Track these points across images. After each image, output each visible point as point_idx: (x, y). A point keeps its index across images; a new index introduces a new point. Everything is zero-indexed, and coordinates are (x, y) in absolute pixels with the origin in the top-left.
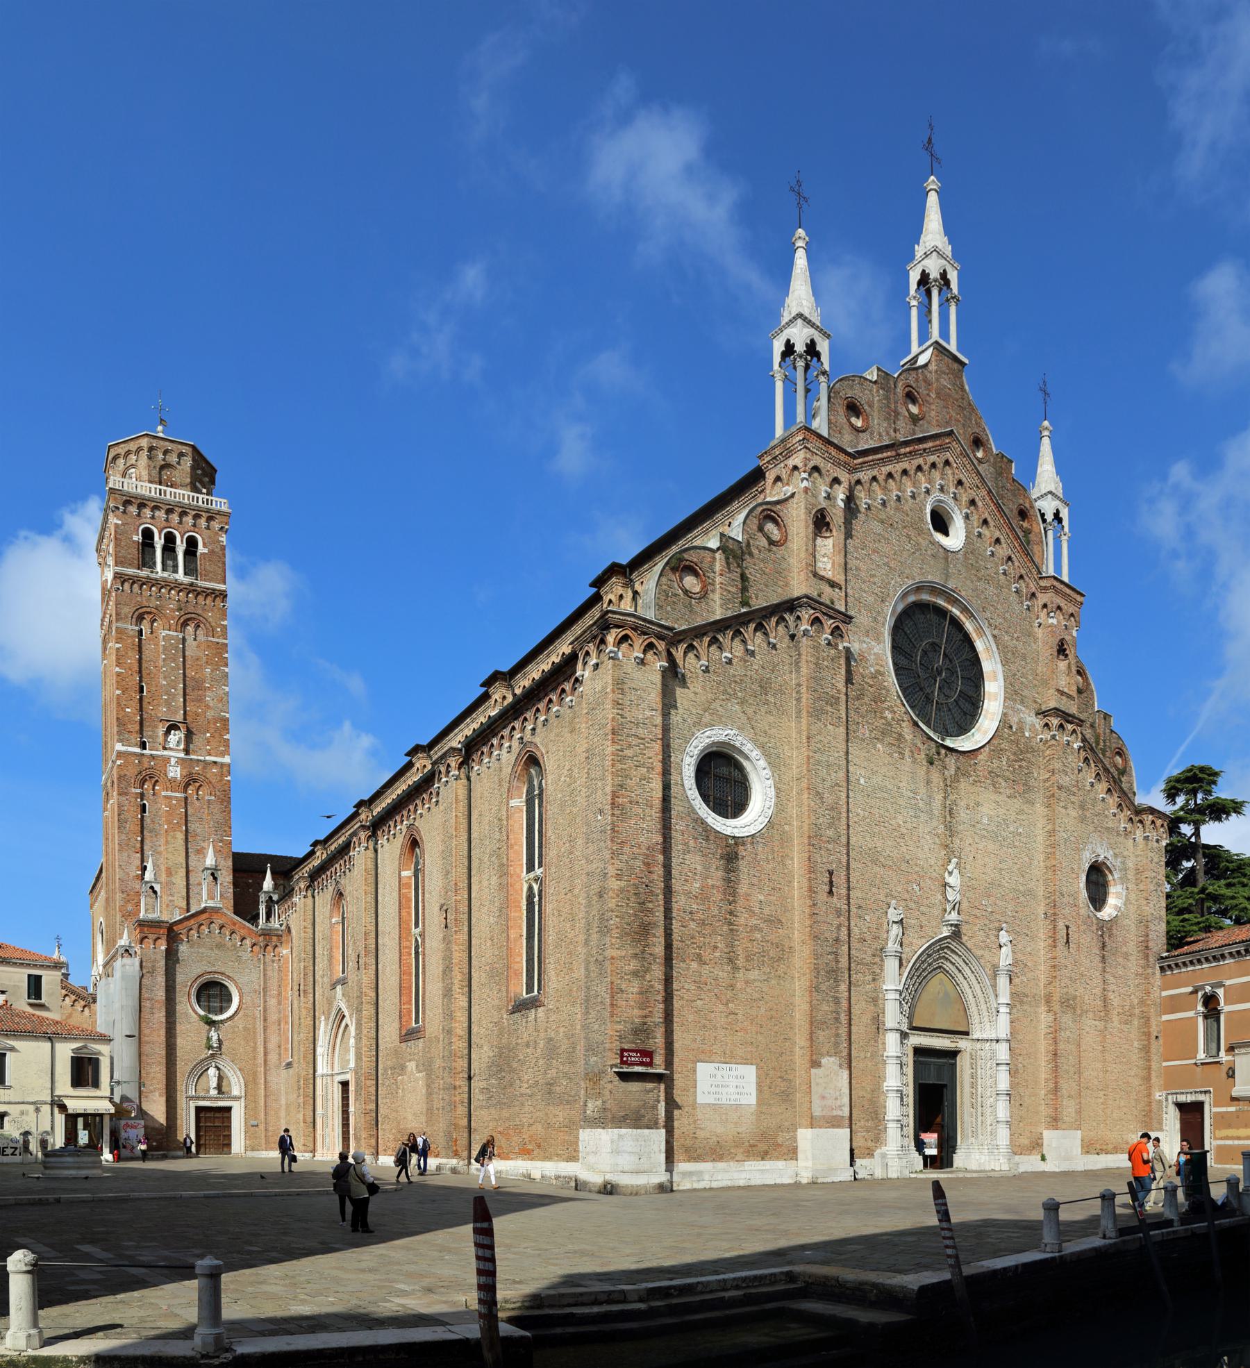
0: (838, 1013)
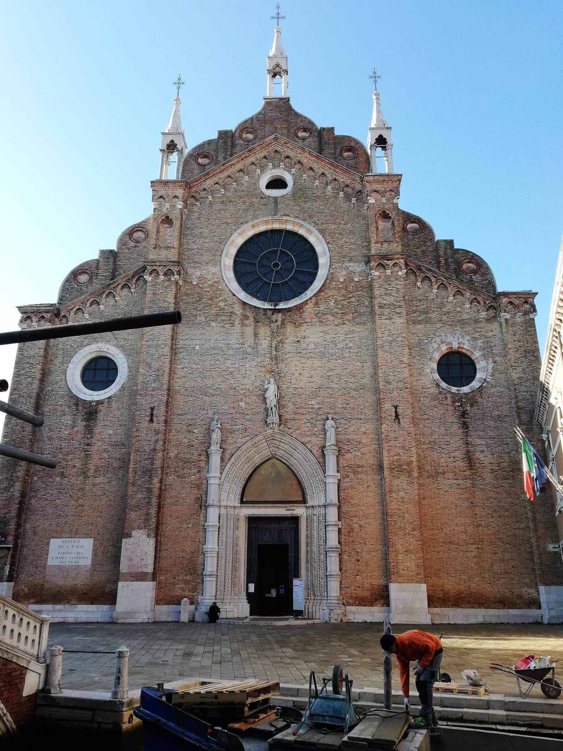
0: (150, 498)
